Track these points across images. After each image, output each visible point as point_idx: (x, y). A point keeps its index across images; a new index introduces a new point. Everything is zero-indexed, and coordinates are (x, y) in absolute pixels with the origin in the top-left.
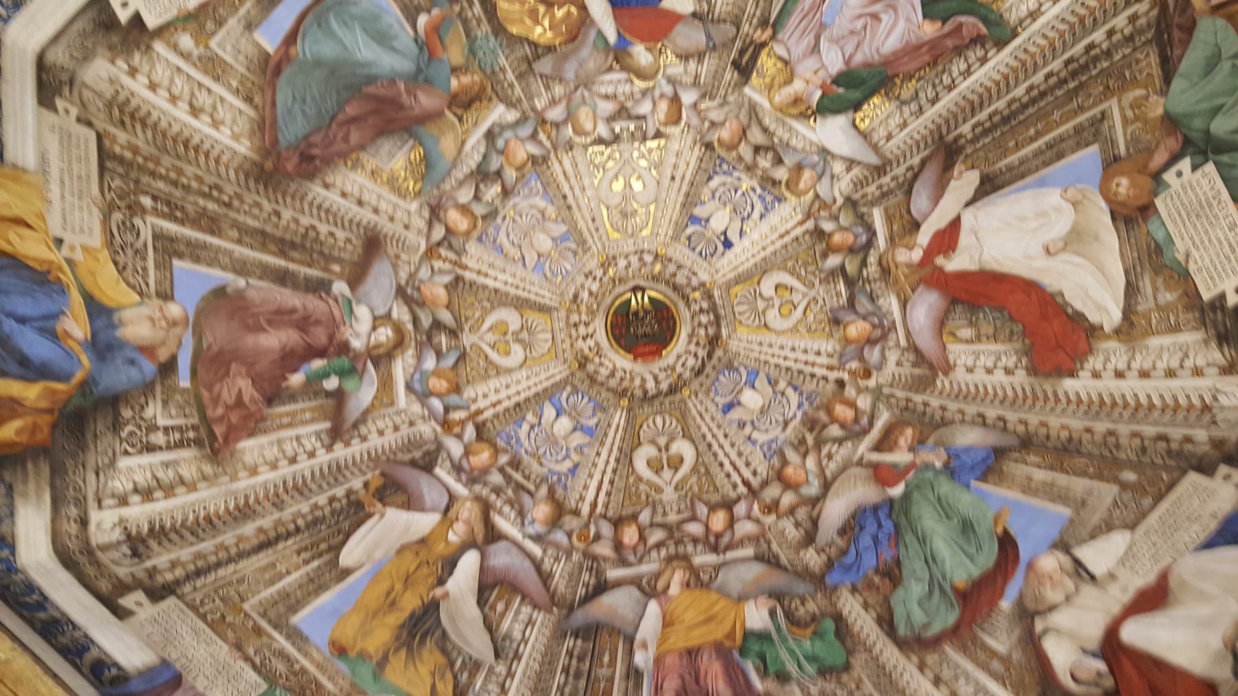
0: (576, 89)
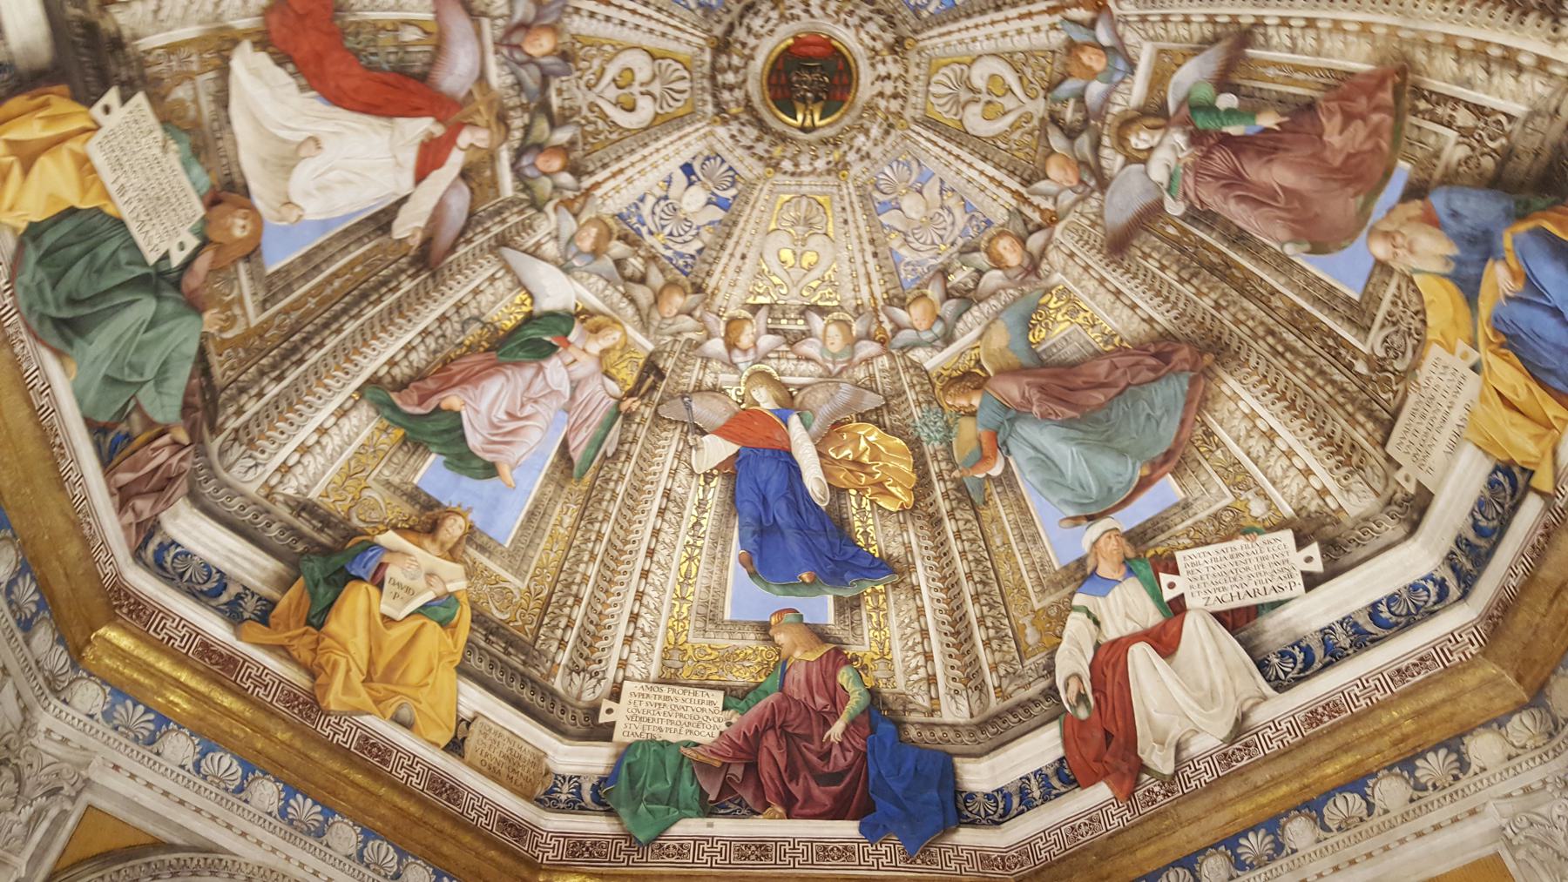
0: (840, 372)
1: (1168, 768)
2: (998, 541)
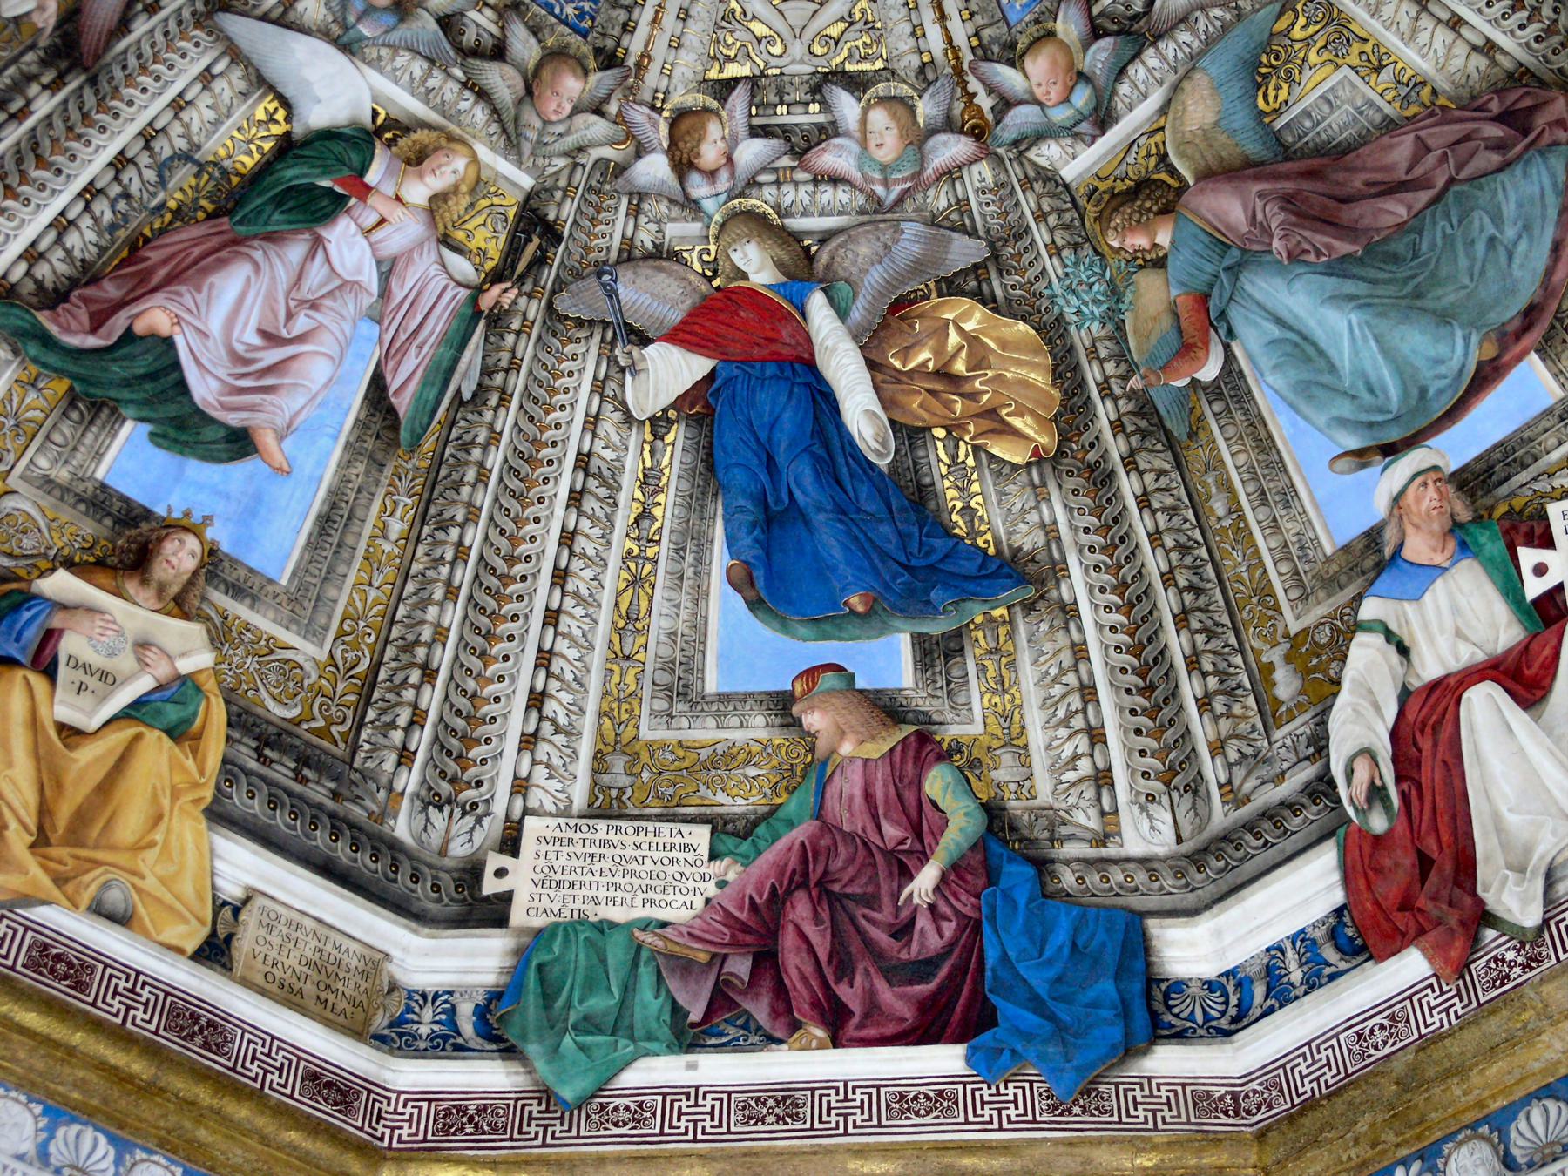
0: (900, 201)
1: (1530, 917)
2: (1219, 507)
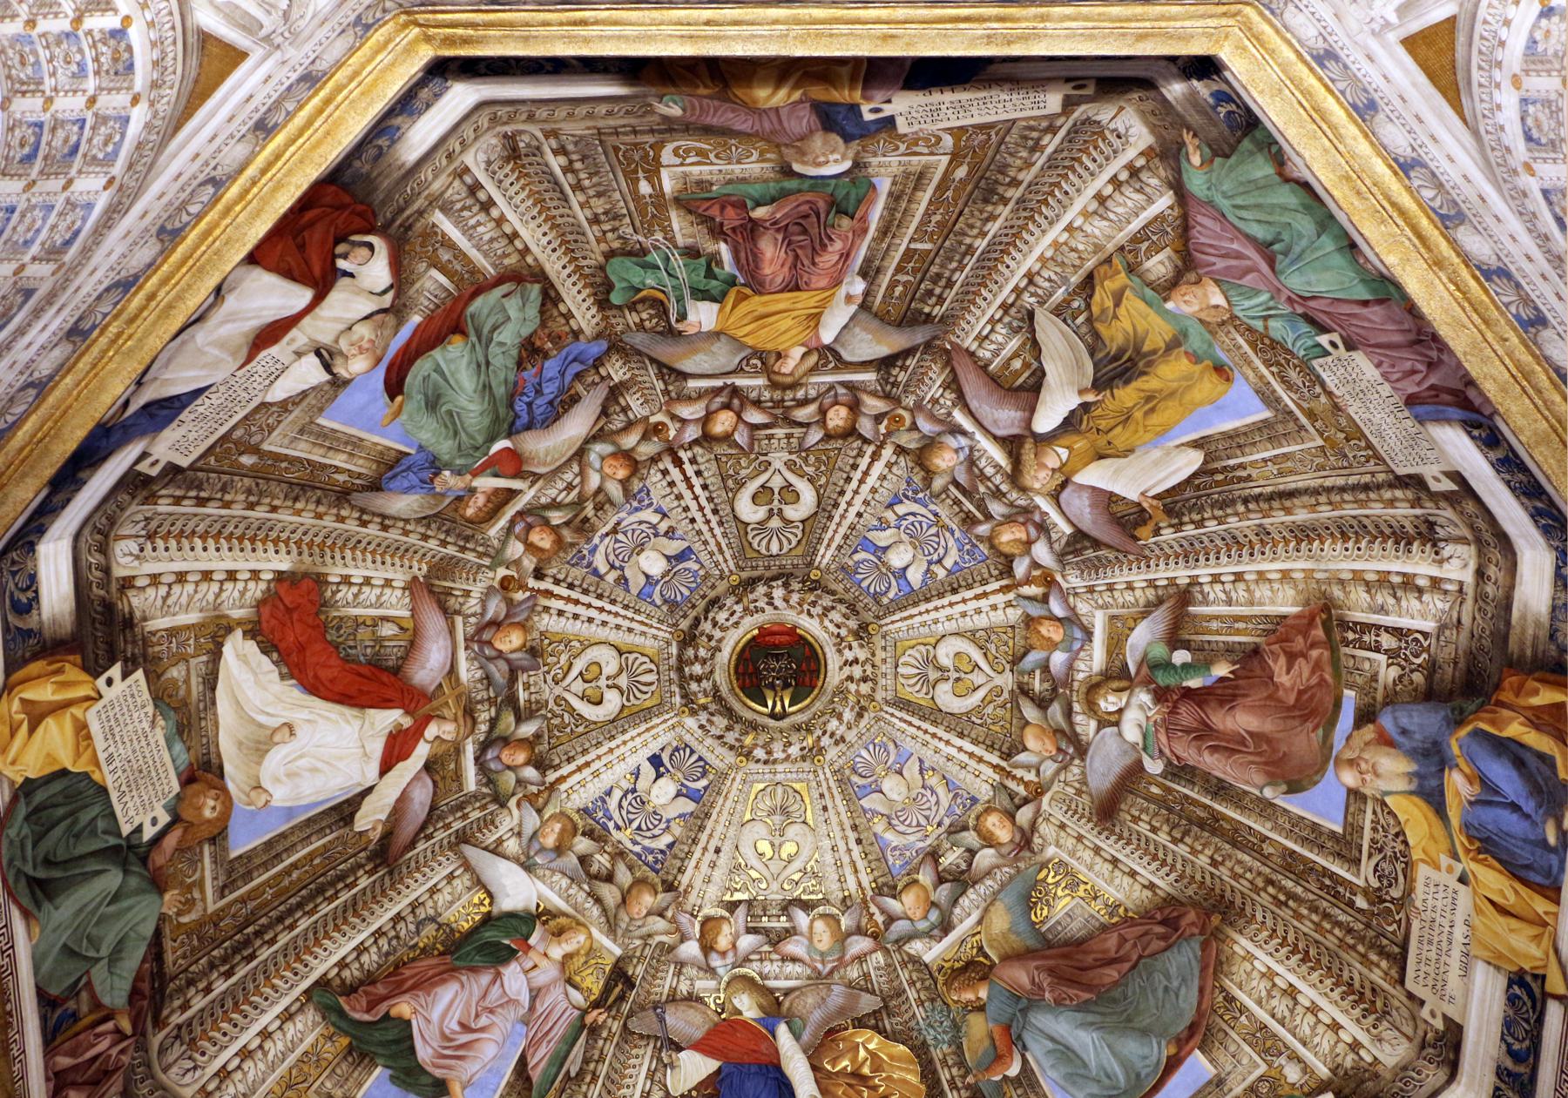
0: (831, 972)
